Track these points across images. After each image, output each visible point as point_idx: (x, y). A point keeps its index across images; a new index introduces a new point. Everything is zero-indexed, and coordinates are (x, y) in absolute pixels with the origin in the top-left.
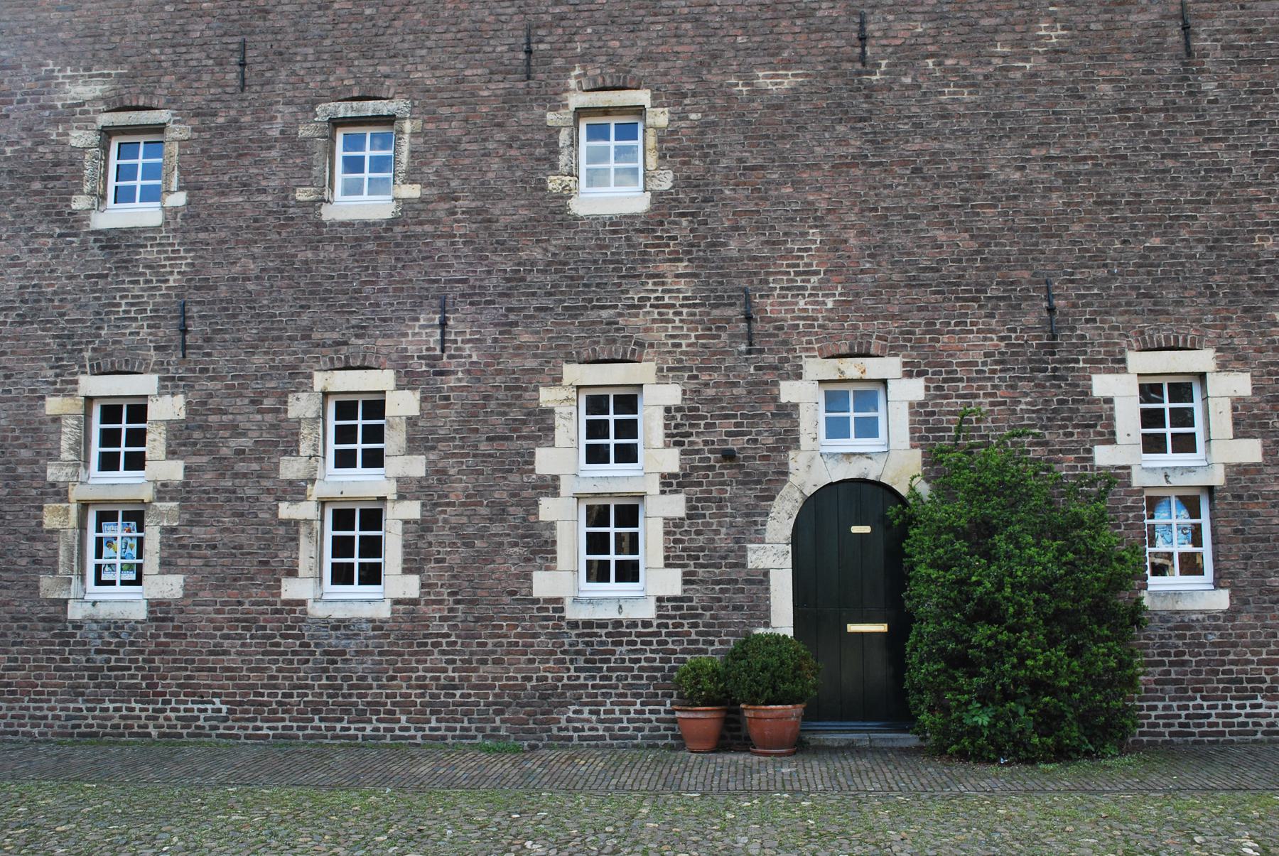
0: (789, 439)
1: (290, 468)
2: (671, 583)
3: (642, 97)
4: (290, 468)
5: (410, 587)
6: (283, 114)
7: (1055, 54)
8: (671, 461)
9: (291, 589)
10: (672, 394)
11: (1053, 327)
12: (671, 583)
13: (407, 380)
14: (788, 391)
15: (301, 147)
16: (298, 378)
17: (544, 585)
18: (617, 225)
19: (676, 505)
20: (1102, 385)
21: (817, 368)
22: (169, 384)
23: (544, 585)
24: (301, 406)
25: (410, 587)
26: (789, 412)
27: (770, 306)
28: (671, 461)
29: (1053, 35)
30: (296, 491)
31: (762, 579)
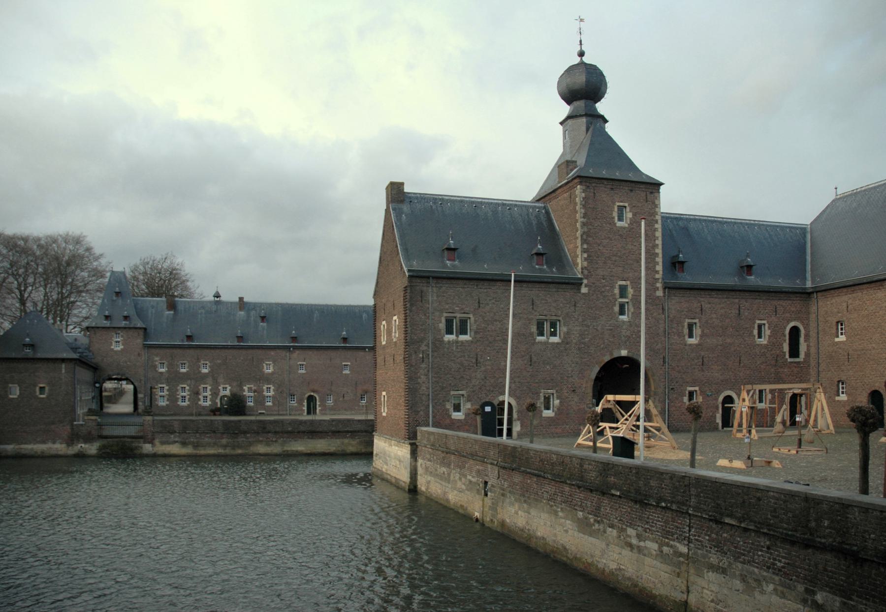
0: (219, 392)
1: (178, 393)
2: (210, 403)
3: (207, 362)
4: (178, 393)
5: (189, 403)
6: (176, 362)
7: (242, 360)
8: (210, 393)
9: (179, 403)
10: (210, 388)
11: (241, 383)
12: (210, 403)
13: (188, 386)
14: (220, 388)
15: (177, 365)
16: (178, 385)
17: (200, 403)
18: (206, 373)
19: (210, 397)
20: (244, 388)
21: (222, 386)
22: (167, 386)
23: (200, 403)
24: (179, 388)
25: (189, 403)
26: (219, 389)
27: (218, 381)
28: (210, 393)
29: (242, 358)
30: (178, 395)
31: (217, 403)
